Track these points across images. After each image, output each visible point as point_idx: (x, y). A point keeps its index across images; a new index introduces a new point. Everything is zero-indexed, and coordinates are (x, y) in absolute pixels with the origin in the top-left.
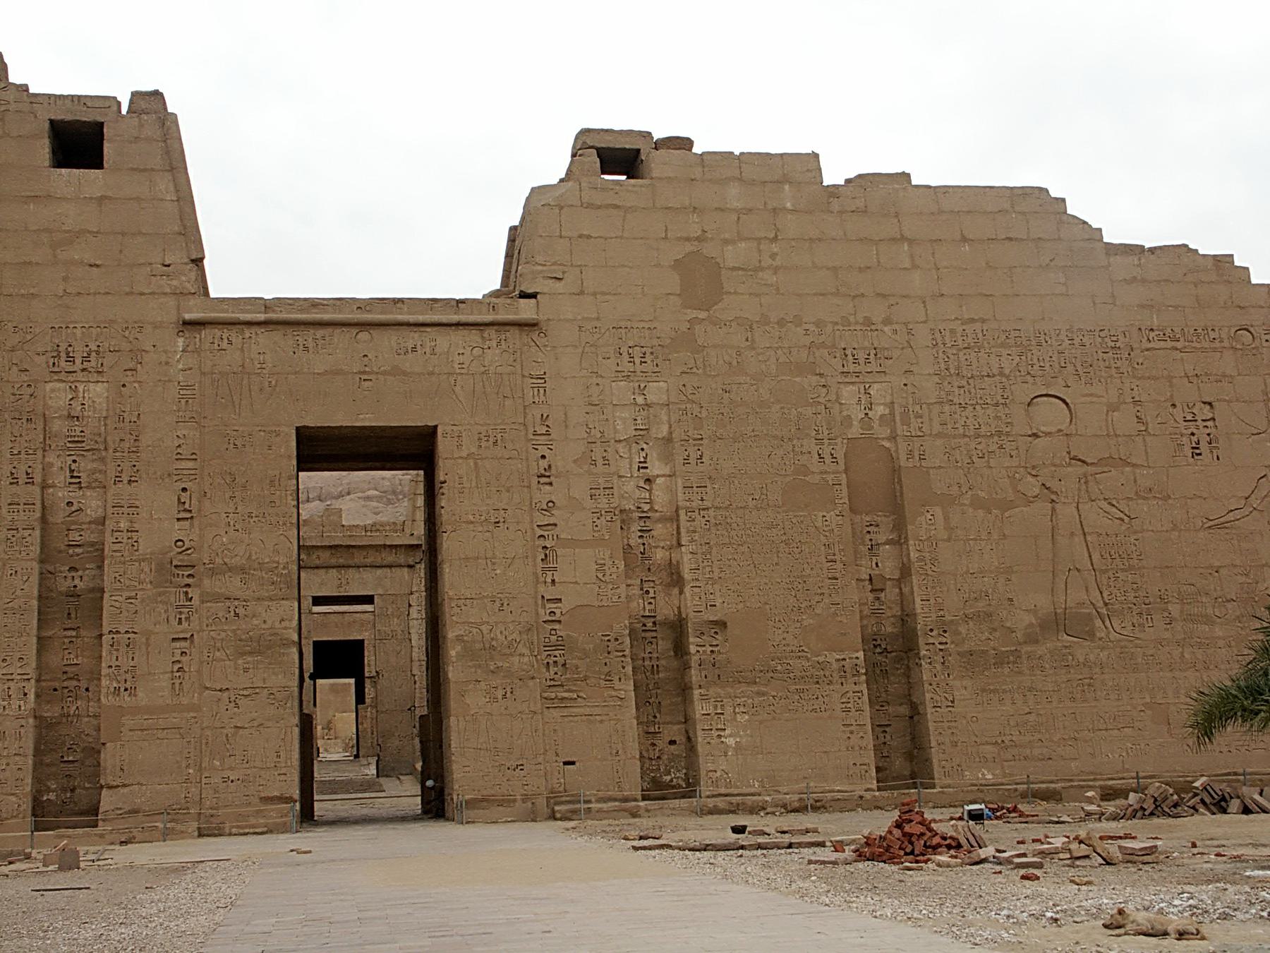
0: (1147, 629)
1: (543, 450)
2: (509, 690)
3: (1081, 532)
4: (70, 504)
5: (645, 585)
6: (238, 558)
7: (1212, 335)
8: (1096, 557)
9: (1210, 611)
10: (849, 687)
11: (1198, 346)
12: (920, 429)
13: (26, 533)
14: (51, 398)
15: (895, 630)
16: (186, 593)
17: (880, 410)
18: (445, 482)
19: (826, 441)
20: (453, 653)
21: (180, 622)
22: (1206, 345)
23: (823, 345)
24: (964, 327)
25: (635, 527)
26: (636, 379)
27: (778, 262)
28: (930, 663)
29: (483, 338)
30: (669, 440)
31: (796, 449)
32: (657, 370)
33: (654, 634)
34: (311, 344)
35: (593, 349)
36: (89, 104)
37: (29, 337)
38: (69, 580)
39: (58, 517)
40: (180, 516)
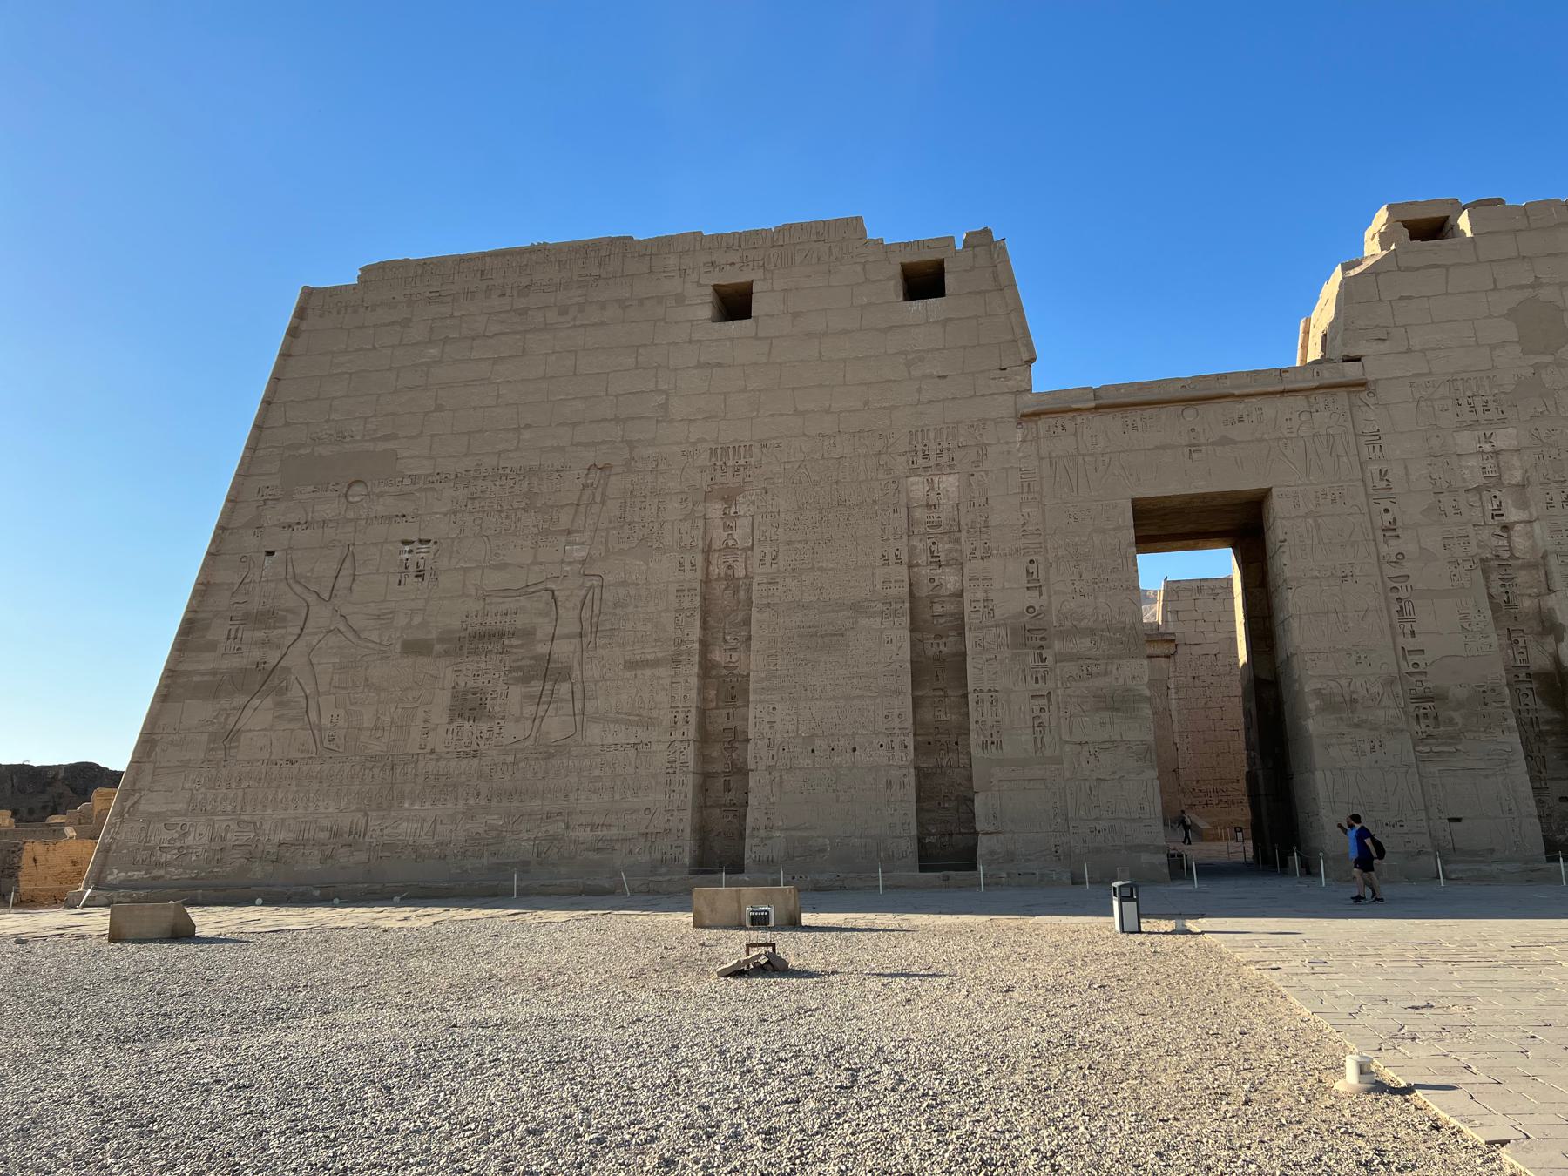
1: (1386, 504)
2: (1377, 744)
4: (932, 580)
5: (1514, 636)
6: (1087, 621)
13: (898, 606)
14: (912, 491)
16: (1040, 655)
18: (1285, 541)
20: (1312, 706)
21: (1037, 682)
25: (1495, 576)
26: (1480, 428)
29: (1309, 402)
30: (1522, 486)
32: (1503, 416)
33: (1530, 686)
34: (1139, 424)
35: (1429, 403)
36: (931, 246)
37: (891, 441)
38: (935, 646)
39: (924, 591)
40: (1029, 585)
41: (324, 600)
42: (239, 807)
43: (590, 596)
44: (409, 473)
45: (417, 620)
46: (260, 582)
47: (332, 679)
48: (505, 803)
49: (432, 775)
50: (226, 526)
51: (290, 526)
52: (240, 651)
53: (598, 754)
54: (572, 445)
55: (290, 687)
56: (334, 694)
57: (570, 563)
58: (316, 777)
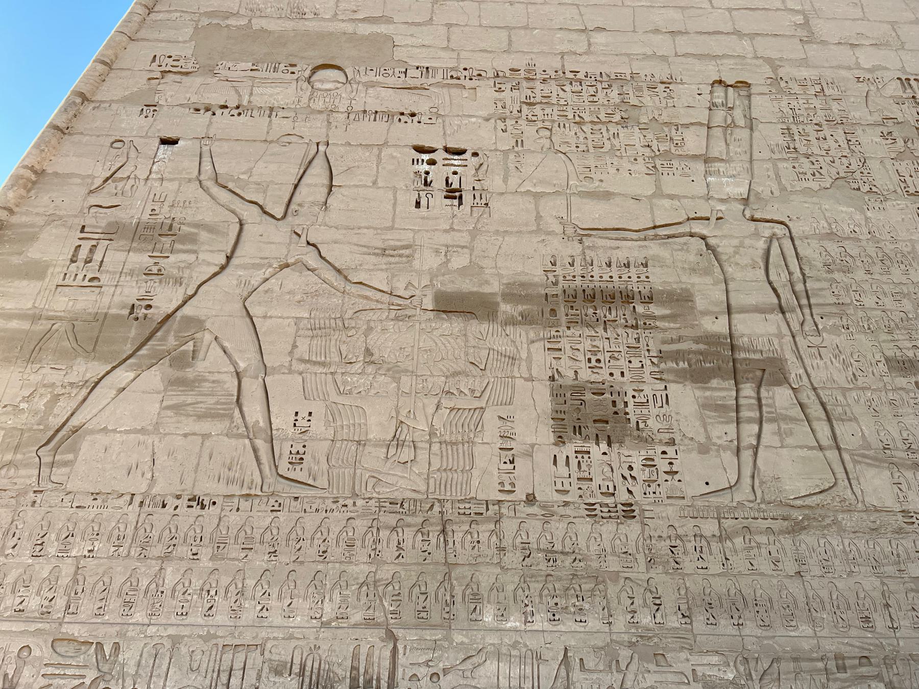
41: (273, 217)
42: (60, 603)
43: (775, 250)
44: (417, 64)
45: (459, 261)
46: (147, 179)
47: (295, 346)
48: (725, 626)
49: (539, 550)
50: (88, 95)
51: (207, 110)
52: (95, 283)
53: (899, 531)
54: (676, 55)
55: (201, 355)
56: (301, 373)
57: (722, 201)
58: (262, 542)
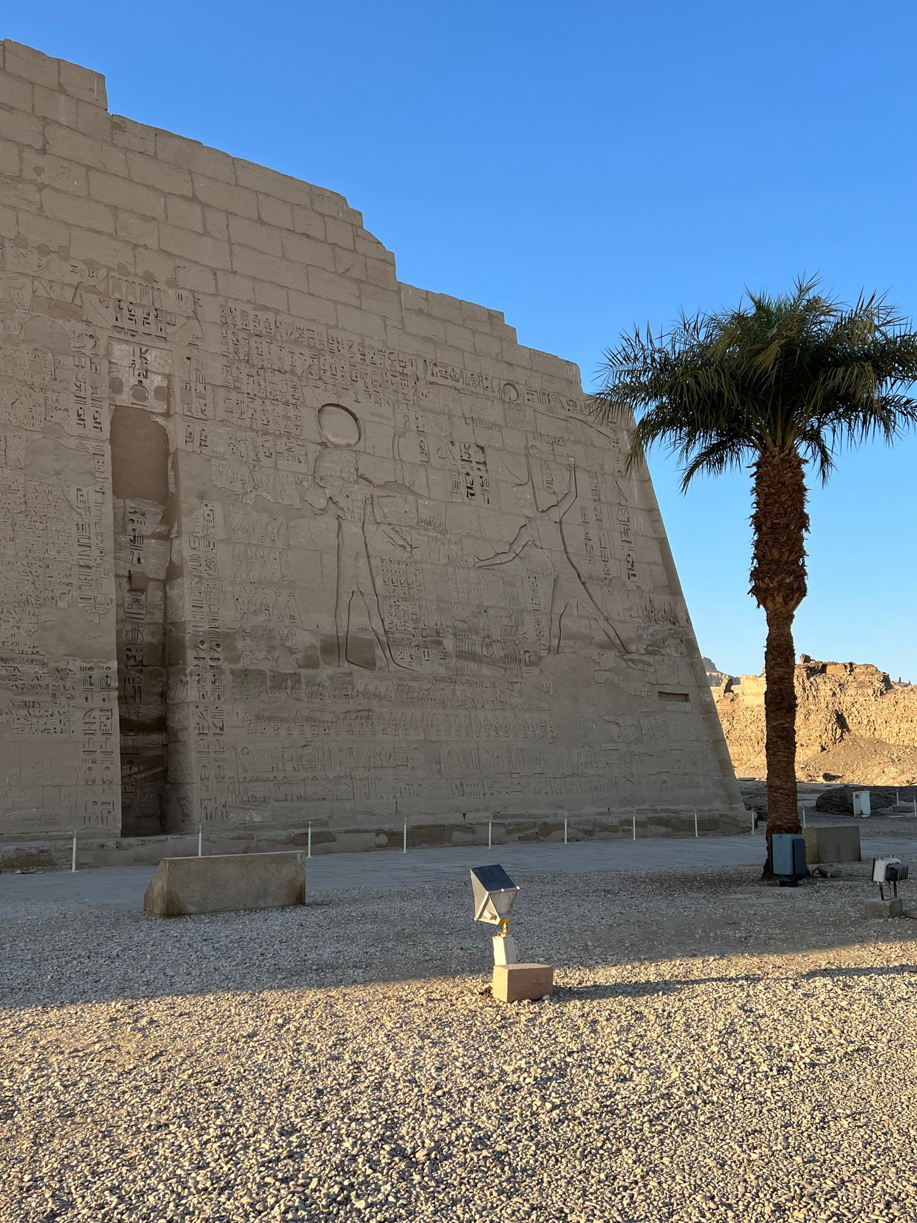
0: (423, 662)
3: (365, 554)
7: (486, 383)
8: (379, 583)
9: (478, 649)
10: (96, 701)
11: (475, 390)
12: (203, 411)
15: (155, 641)
17: (156, 381)
19: (89, 402)
22: (480, 390)
23: (92, 290)
24: (257, 313)
27: (44, 178)
28: (199, 681)
31: (49, 403)
